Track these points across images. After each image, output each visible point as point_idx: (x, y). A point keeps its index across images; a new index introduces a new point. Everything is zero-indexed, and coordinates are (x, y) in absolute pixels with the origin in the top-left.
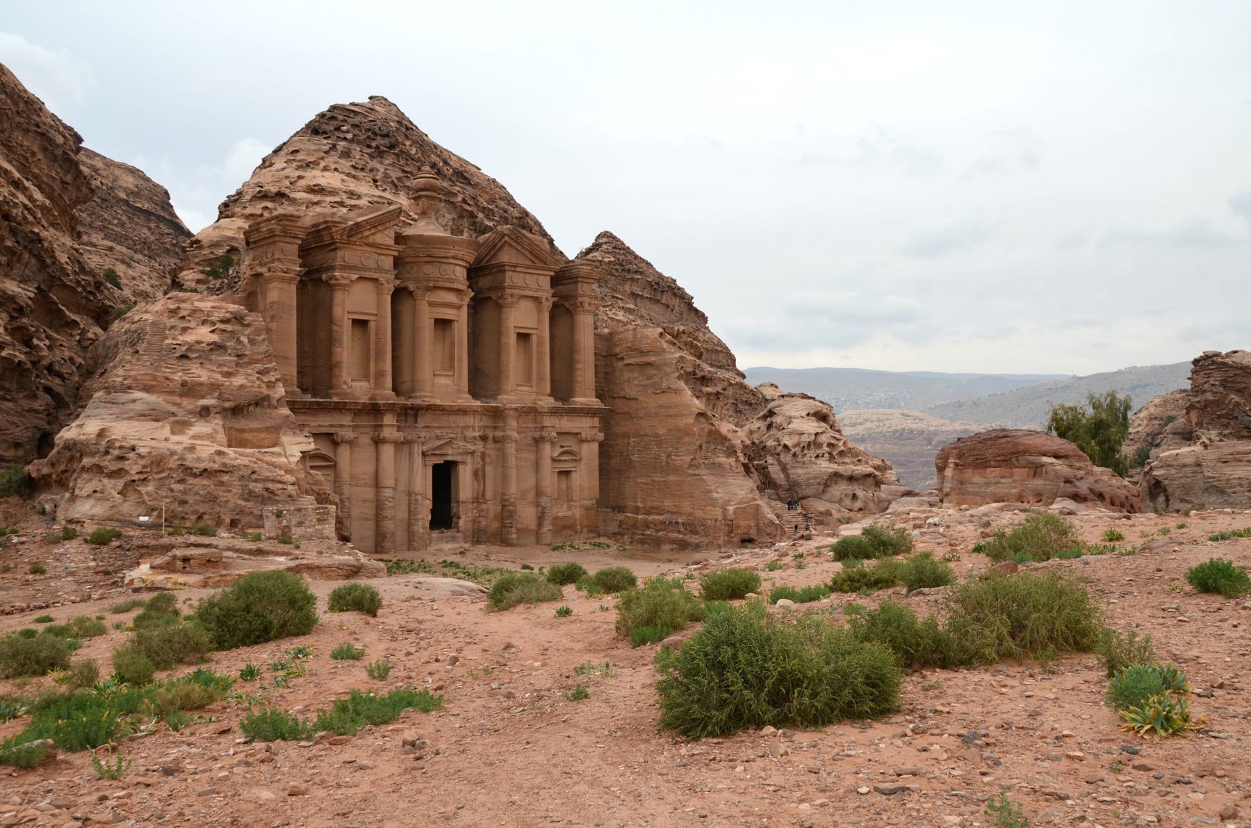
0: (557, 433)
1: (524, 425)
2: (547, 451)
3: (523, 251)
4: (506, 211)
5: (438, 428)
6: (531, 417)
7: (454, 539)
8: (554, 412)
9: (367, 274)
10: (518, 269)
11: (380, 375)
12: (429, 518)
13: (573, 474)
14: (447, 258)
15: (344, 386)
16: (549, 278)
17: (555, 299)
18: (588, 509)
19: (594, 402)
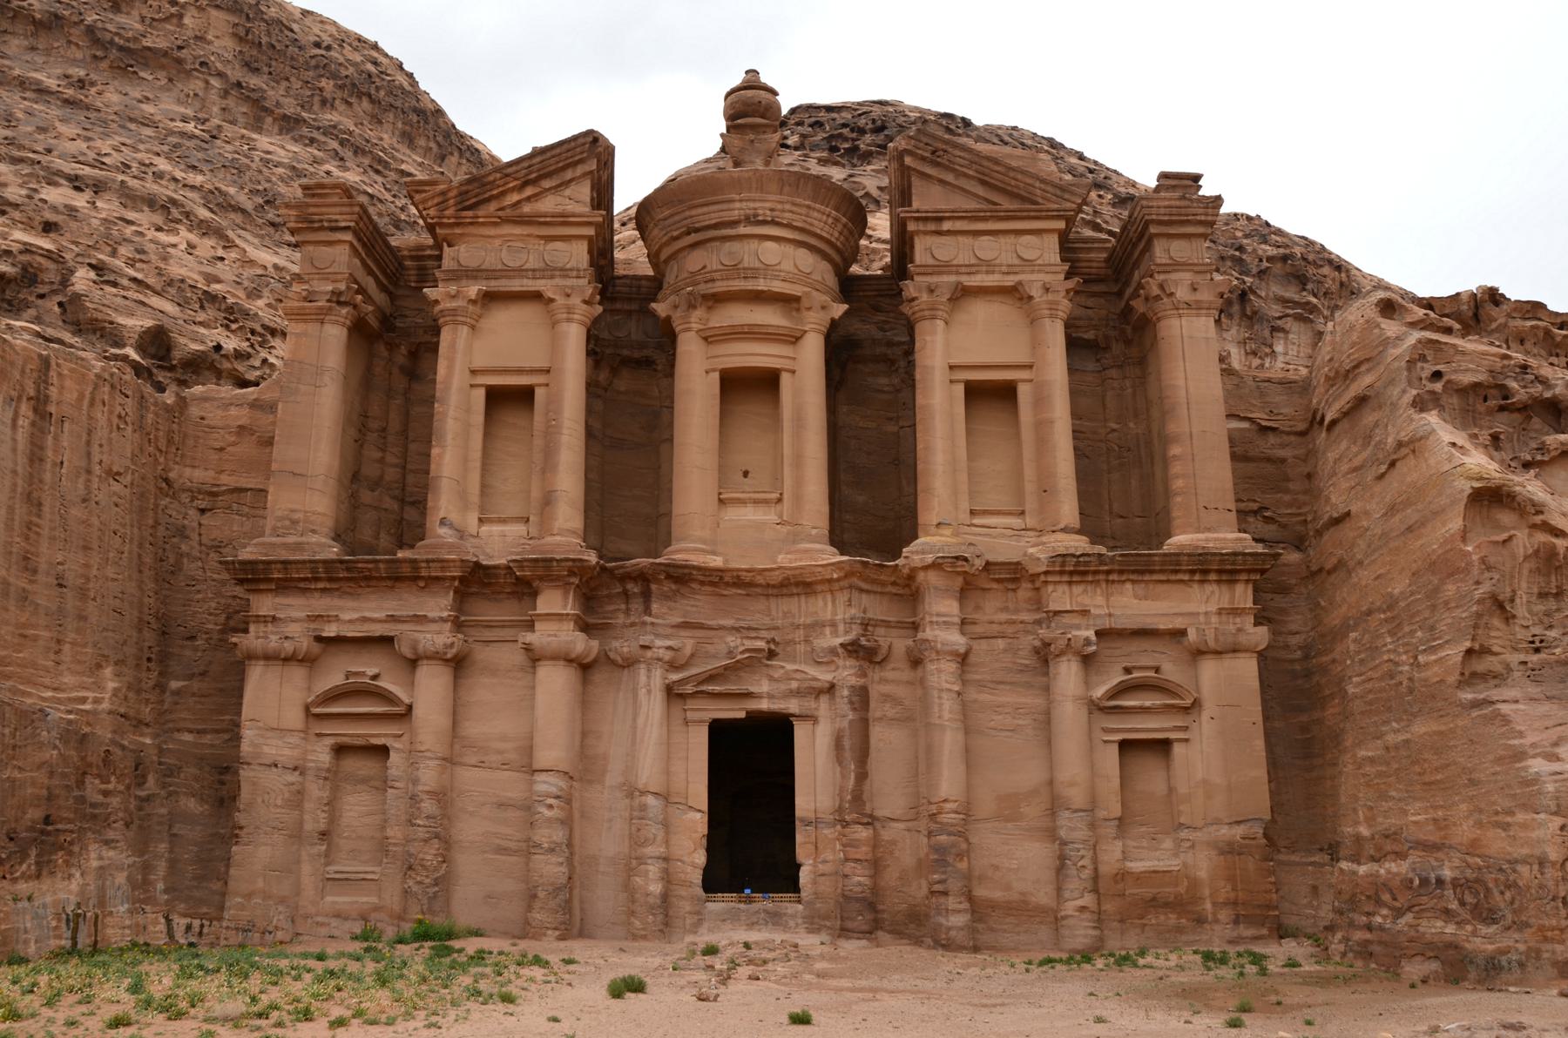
0: (1097, 633)
1: (1003, 617)
2: (1068, 674)
3: (963, 183)
4: (1241, 248)
5: (737, 629)
6: (1024, 592)
7: (775, 919)
8: (1074, 570)
9: (516, 285)
10: (946, 226)
11: (548, 501)
12: (701, 858)
13: (1177, 749)
14: (734, 224)
15: (443, 531)
16: (1053, 242)
17: (1071, 284)
18: (1229, 850)
19: (1228, 538)
